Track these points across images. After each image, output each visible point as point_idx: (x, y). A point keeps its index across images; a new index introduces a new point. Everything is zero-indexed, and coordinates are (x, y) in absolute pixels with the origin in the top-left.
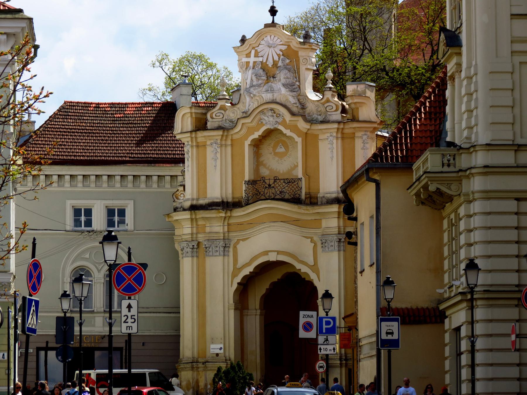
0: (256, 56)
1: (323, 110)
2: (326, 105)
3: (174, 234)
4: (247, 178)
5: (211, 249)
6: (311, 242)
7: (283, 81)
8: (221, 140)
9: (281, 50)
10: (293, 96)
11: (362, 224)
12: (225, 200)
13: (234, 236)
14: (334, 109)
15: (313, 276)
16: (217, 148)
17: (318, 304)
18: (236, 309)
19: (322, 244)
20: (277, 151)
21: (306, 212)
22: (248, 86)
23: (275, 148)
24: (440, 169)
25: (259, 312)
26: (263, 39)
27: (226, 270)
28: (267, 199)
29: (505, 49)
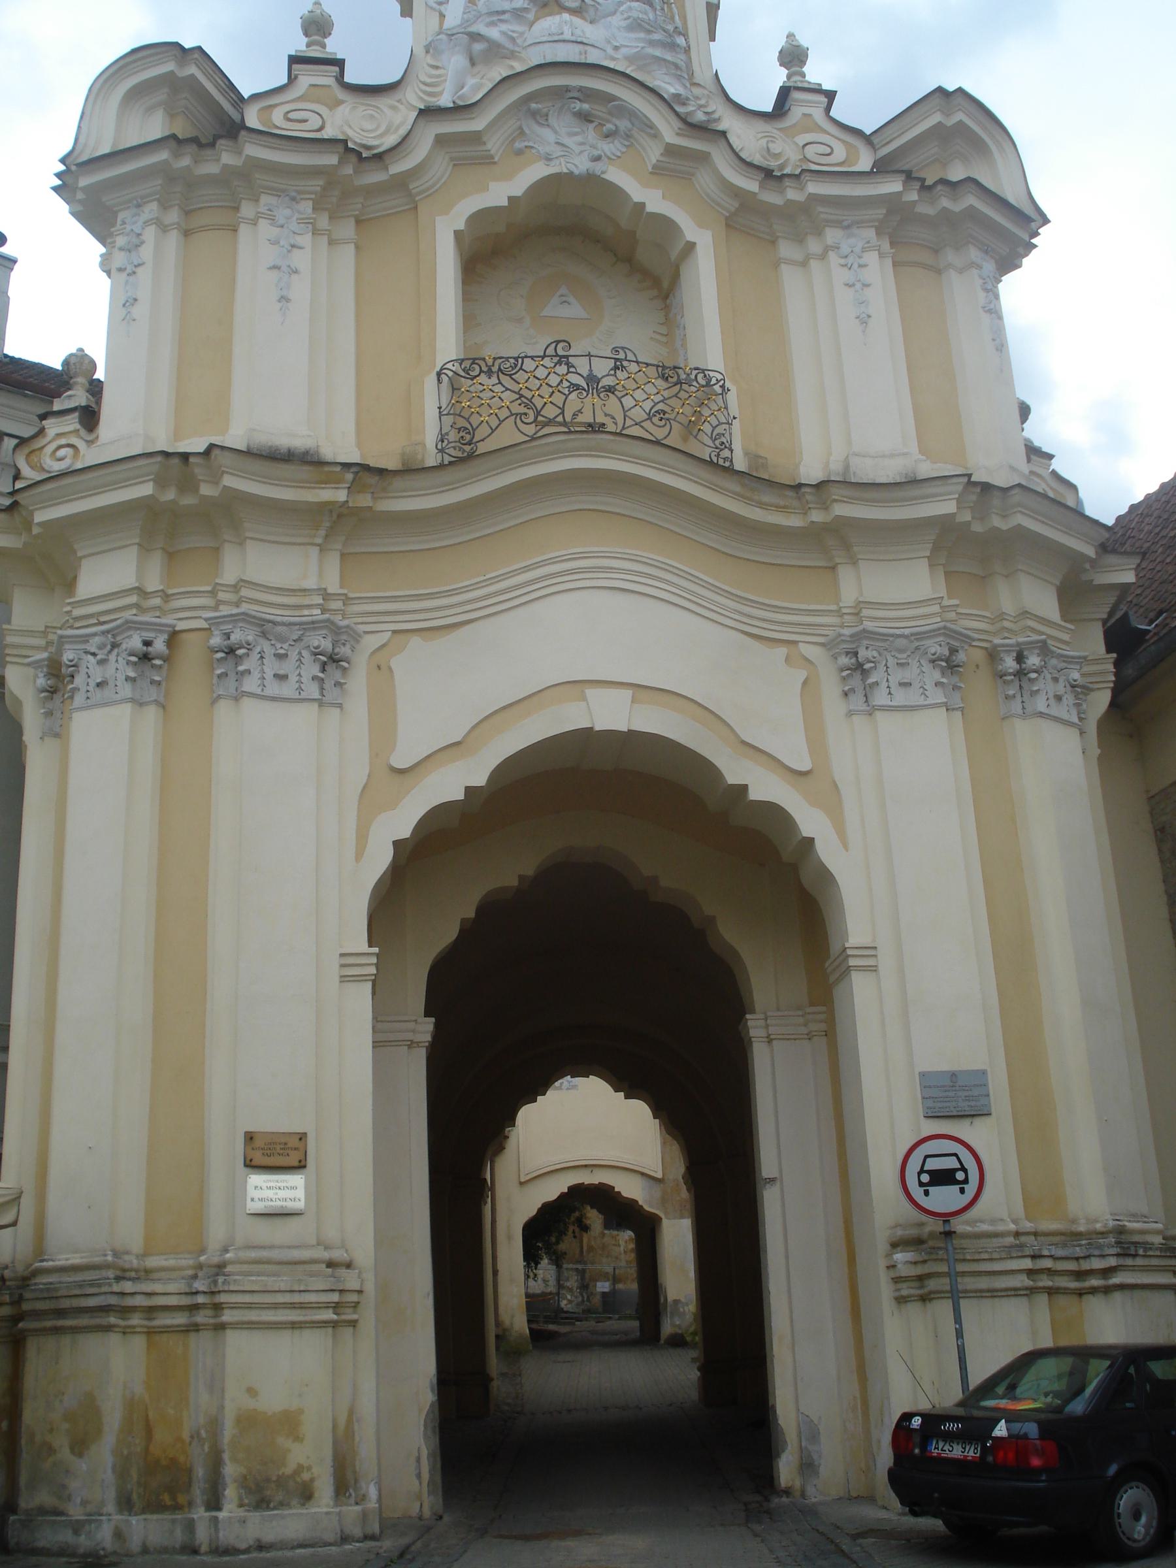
2: (802, 139)
6: (787, 660)
17: (852, 962)
25: (426, 1029)
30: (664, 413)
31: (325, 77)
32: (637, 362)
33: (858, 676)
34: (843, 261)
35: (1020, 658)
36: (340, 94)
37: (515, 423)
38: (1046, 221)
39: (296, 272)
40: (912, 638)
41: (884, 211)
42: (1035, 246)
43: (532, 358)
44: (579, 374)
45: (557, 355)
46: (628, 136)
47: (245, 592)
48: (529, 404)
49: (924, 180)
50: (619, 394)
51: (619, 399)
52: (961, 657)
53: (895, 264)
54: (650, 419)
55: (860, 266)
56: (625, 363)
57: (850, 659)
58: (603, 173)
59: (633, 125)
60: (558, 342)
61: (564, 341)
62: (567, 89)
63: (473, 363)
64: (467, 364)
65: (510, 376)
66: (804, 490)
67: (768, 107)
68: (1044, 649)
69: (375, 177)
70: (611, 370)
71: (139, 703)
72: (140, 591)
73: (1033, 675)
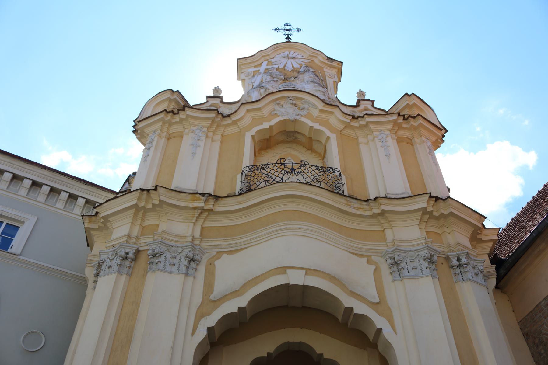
0: (270, 63)
5: (162, 259)
6: (368, 262)
8: (209, 128)
10: (323, 92)
15: (379, 322)
16: (200, 134)
21: (358, 212)
26: (280, 54)
30: (318, 179)
31: (217, 101)
32: (309, 165)
33: (395, 266)
34: (379, 140)
35: (459, 260)
37: (265, 183)
38: (446, 131)
39: (199, 146)
40: (415, 252)
41: (392, 126)
42: (444, 141)
43: (272, 164)
44: (288, 168)
45: (281, 163)
46: (308, 110)
49: (404, 116)
50: (302, 174)
51: (302, 175)
53: (397, 143)
54: (313, 181)
55: (385, 142)
56: (304, 165)
57: (392, 260)
58: (300, 119)
59: (309, 106)
60: (281, 159)
61: (284, 158)
63: (252, 167)
64: (250, 167)
65: (265, 170)
66: (370, 201)
67: (355, 104)
70: (300, 167)
73: (465, 266)
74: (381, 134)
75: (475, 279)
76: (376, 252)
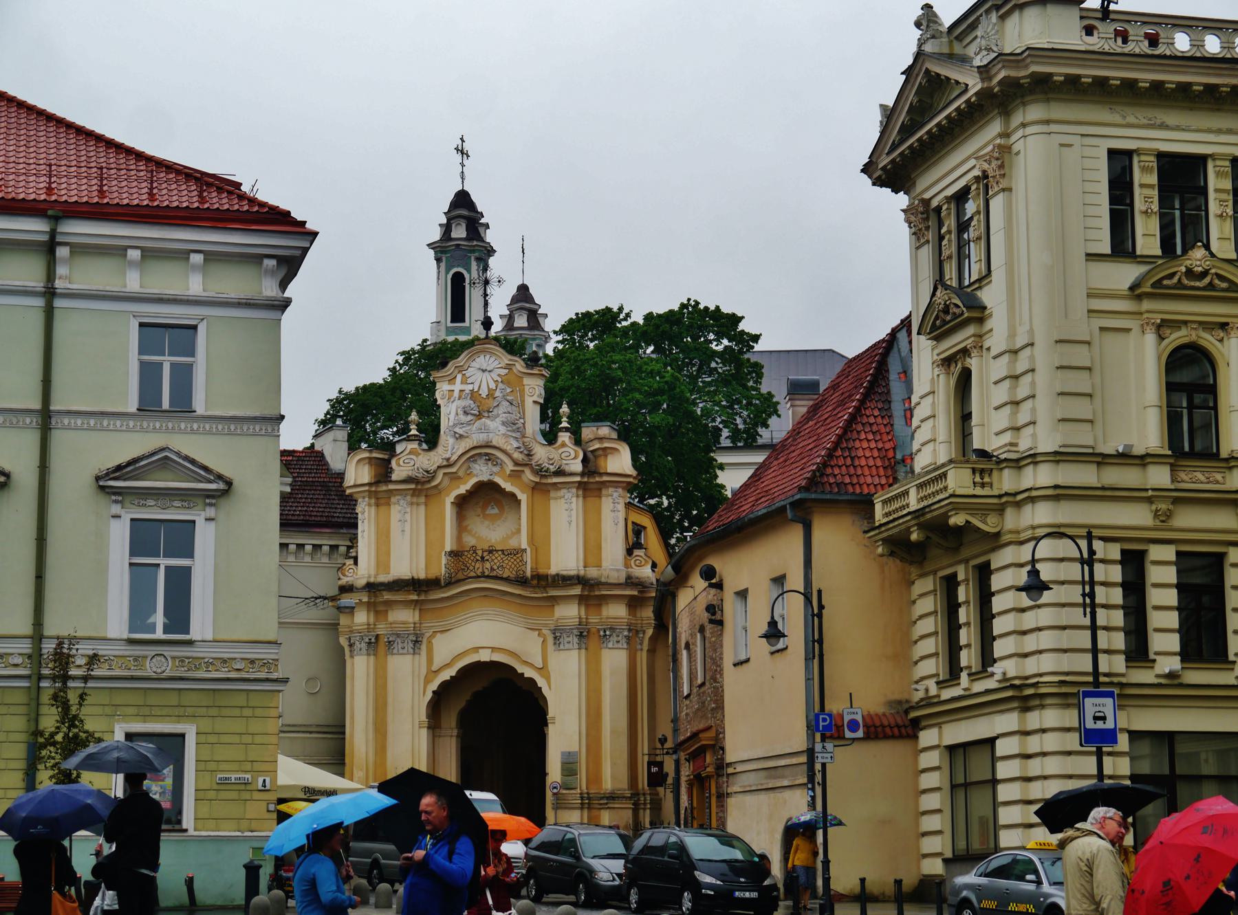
0: (464, 382)
1: (557, 457)
2: (560, 451)
3: (339, 624)
4: (448, 548)
6: (539, 635)
7: (503, 417)
9: (499, 375)
11: (743, 594)
12: (416, 577)
13: (430, 625)
14: (573, 455)
15: (541, 682)
18: (428, 728)
19: (555, 638)
20: (487, 512)
22: (451, 424)
23: (484, 507)
24: (970, 492)
25: (455, 732)
27: (416, 673)
28: (479, 577)
29: (1080, 305)
35: (605, 632)
36: (420, 452)
47: (393, 625)
48: (466, 566)
52: (585, 633)
62: (480, 453)
68: (610, 628)
69: (428, 486)
71: (368, 655)
72: (368, 625)
74: (569, 492)
75: (616, 646)
76: (546, 625)
